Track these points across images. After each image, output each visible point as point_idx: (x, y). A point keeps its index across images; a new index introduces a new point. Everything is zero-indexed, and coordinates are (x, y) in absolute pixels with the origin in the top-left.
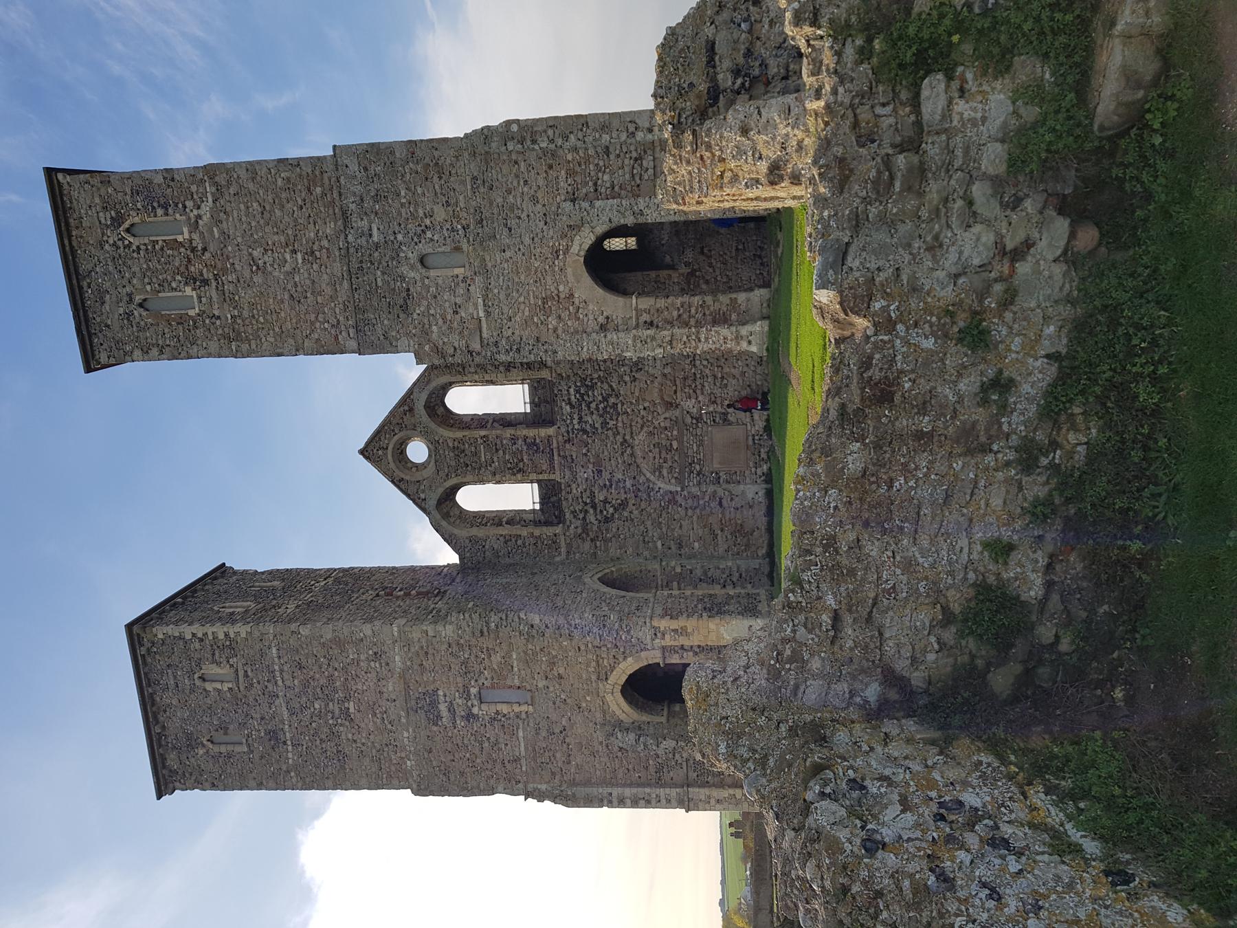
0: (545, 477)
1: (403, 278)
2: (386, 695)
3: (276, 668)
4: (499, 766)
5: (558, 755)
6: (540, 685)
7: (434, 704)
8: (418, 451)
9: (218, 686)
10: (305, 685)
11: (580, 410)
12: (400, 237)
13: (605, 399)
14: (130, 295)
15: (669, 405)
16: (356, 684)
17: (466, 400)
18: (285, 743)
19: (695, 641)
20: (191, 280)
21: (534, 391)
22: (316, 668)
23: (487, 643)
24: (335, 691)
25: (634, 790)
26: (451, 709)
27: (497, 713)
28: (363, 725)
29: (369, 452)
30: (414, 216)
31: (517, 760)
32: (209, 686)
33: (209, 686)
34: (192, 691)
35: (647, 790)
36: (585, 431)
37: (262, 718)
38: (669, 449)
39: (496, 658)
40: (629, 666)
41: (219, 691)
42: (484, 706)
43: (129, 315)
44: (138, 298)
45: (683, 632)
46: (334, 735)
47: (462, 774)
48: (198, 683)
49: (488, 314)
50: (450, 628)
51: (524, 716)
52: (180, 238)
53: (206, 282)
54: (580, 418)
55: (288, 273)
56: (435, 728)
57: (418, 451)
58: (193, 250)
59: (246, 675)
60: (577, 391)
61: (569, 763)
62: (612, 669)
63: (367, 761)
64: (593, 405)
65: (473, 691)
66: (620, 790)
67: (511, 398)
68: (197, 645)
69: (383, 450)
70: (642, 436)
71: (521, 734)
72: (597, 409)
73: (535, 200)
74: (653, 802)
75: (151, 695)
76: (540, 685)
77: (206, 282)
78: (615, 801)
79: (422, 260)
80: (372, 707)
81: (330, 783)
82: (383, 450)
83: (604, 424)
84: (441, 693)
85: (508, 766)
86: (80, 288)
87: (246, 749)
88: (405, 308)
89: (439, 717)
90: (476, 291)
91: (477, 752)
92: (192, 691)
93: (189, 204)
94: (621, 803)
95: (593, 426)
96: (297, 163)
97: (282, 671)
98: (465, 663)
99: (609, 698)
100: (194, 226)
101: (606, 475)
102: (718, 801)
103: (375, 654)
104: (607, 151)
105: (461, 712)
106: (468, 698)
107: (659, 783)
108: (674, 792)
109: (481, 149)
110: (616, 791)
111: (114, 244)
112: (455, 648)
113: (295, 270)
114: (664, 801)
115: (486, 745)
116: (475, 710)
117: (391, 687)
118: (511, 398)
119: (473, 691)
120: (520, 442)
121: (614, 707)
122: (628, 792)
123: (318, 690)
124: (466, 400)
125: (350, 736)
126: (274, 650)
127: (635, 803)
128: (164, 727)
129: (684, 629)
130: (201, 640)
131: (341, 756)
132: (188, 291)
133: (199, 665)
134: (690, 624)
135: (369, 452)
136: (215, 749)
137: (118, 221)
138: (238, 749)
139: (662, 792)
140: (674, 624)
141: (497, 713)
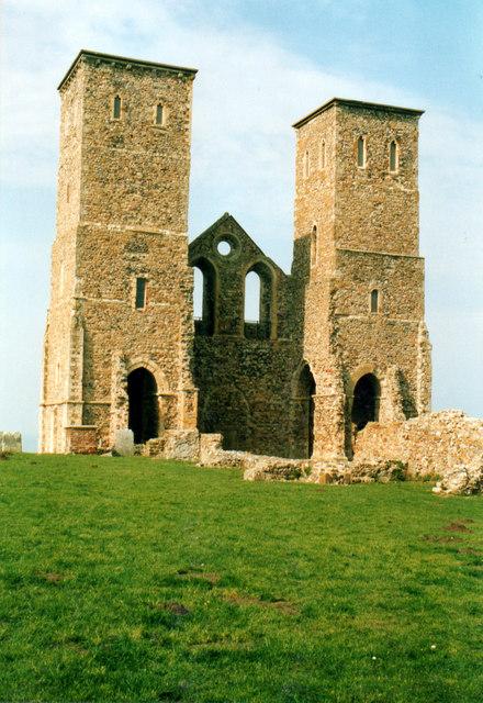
0: (216, 329)
1: (369, 280)
6: (149, 318)
7: (137, 249)
8: (224, 248)
9: (155, 115)
11: (254, 354)
13: (259, 370)
15: (253, 406)
17: (252, 283)
18: (115, 146)
20: (370, 169)
21: (258, 326)
22: (164, 179)
23: (176, 288)
24: (149, 188)
25: (81, 369)
26: (134, 259)
27: (131, 288)
29: (227, 221)
31: (99, 295)
32: (155, 108)
34: (152, 97)
35: (81, 377)
36: (242, 355)
38: (227, 404)
41: (152, 114)
42: (135, 280)
44: (364, 137)
45: (190, 407)
48: (158, 102)
51: (129, 304)
53: (369, 176)
57: (224, 248)
59: (161, 135)
60: (264, 354)
67: (252, 313)
68: (181, 109)
69: (226, 227)
70: (235, 390)
75: (151, 70)
76: (149, 318)
78: (74, 356)
82: (226, 227)
83: (245, 368)
85: (96, 289)
88: (355, 278)
89: (130, 251)
92: (152, 97)
94: (74, 360)
95: (244, 360)
101: (215, 365)
105: (133, 265)
106: (142, 272)
108: (79, 393)
110: (80, 357)
111: (388, 134)
116: (133, 274)
117: (148, 226)
118: (252, 313)
119: (146, 276)
120: (236, 315)
122: (80, 365)
124: (252, 283)
126: (175, 156)
127: (74, 369)
131: (105, 182)
132: (365, 166)
133: (170, 106)
135: (227, 221)
136: (113, 100)
137: (398, 139)
138: (112, 114)
139: (80, 386)
141: (131, 288)
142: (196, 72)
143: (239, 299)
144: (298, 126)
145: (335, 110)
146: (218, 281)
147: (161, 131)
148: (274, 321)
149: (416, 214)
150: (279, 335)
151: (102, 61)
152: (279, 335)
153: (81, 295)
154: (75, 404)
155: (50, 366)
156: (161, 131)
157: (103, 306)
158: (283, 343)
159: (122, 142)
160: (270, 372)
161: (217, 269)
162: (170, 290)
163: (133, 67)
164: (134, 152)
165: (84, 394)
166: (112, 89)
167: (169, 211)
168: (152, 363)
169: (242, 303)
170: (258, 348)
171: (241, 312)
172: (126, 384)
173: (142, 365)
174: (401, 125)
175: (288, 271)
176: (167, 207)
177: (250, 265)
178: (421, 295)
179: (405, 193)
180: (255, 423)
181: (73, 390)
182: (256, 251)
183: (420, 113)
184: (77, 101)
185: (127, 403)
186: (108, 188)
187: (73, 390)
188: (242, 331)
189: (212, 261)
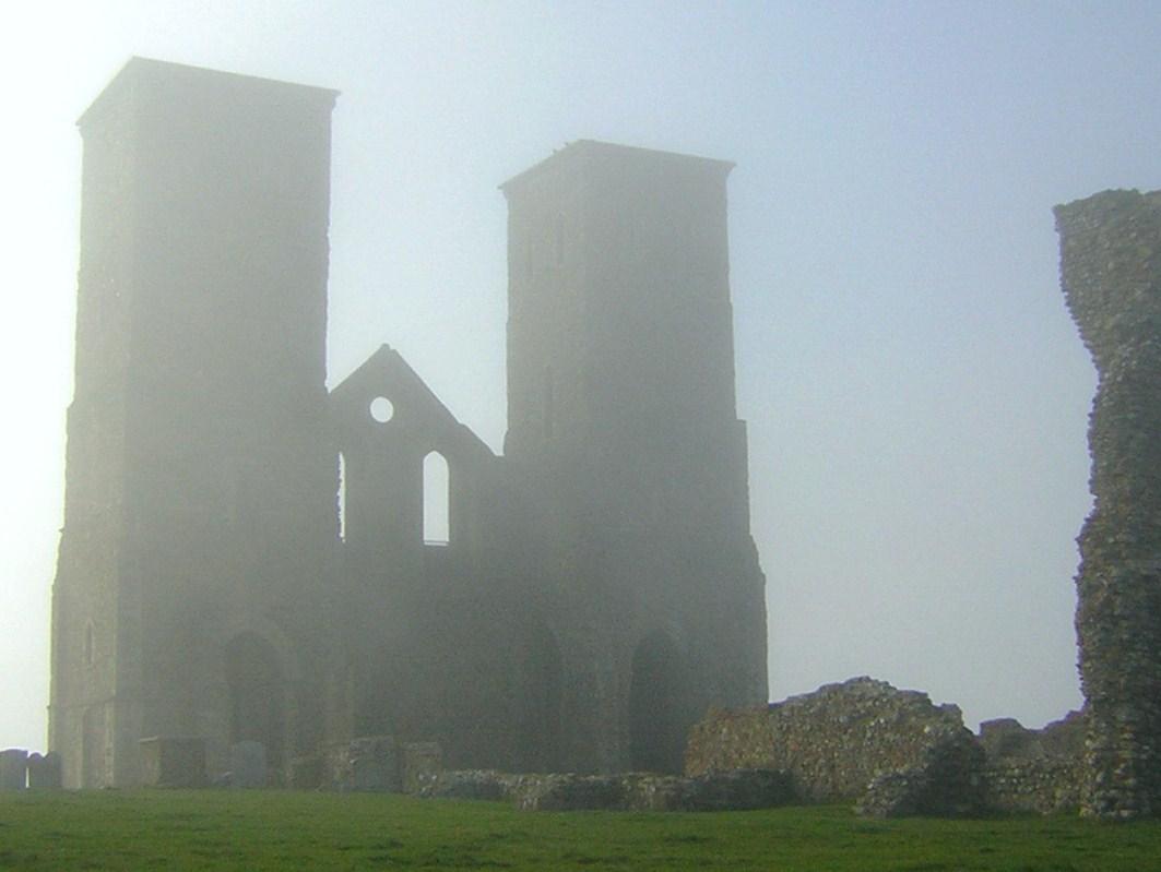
8: (382, 410)
17: (436, 471)
57: (382, 410)
67: (436, 527)
69: (387, 371)
82: (387, 371)
118: (436, 527)
124: (436, 471)
175: (498, 451)
182: (443, 415)
183: (734, 165)
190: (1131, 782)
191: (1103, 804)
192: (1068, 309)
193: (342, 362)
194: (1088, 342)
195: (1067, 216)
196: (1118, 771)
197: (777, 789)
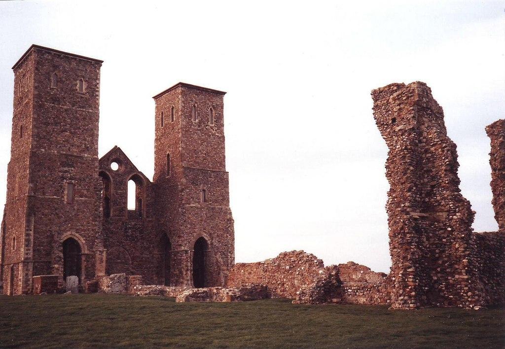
0: (111, 215)
1: (200, 184)
2: (71, 147)
3: (84, 110)
4: (42, 186)
5: (47, 211)
8: (115, 166)
10: (77, 118)
12: (209, 185)
14: (197, 103)
16: (76, 137)
17: (132, 186)
18: (53, 103)
19: (98, 266)
20: (200, 122)
23: (92, 189)
24: (75, 129)
25: (32, 240)
26: (66, 171)
27: (64, 189)
28: (59, 136)
30: (214, 191)
31: (44, 194)
32: (78, 82)
33: (78, 82)
35: (32, 245)
37: (64, 98)
39: (85, 192)
40: (82, 241)
41: (76, 85)
43: (192, 100)
44: (196, 105)
46: (56, 124)
47: (39, 171)
49: (192, 207)
50: (97, 176)
51: (63, 199)
52: (209, 123)
53: (199, 126)
54: (130, 228)
55: (201, 151)
56: (59, 164)
57: (115, 166)
58: (207, 125)
59: (81, 97)
61: (43, 215)
62: (81, 235)
63: (44, 134)
64: (134, 233)
65: (73, 181)
66: (32, 234)
67: (131, 205)
68: (94, 83)
69: (117, 154)
71: (55, 197)
72: (133, 234)
73: (217, 224)
74: (27, 248)
75: (75, 59)
76: (76, 207)
77: (199, 126)
79: (204, 191)
80: (67, 141)
81: (36, 116)
82: (117, 154)
83: (127, 236)
84: (72, 169)
86: (199, 90)
87: (52, 87)
88: (193, 183)
90: (197, 205)
91: (49, 178)
93: (216, 128)
94: (28, 235)
96: (225, 161)
97: (83, 111)
98: (84, 180)
99: (69, 233)
100: (212, 128)
102: (27, 274)
103: (88, 147)
104: (226, 245)
106: (70, 179)
107: (34, 251)
108: (30, 256)
109: (229, 212)
110: (32, 233)
112: (90, 177)
113: (202, 153)
114: (27, 252)
115: (51, 183)
116: (65, 181)
117: (75, 151)
118: (131, 205)
119: (73, 181)
120: (123, 205)
121: (65, 234)
122: (32, 238)
123: (74, 123)
124: (132, 186)
125: (56, 130)
127: (27, 240)
128: (61, 58)
129: (102, 262)
130: (96, 86)
132: (197, 121)
134: (104, 264)
137: (213, 106)
139: (31, 251)
140: (104, 259)
141: (64, 189)
142: (102, 62)
143: (124, 196)
144: (155, 98)
145: (179, 90)
146: (112, 186)
147: (82, 95)
148: (144, 208)
149: (223, 148)
150: (148, 217)
151: (45, 52)
152: (148, 217)
153: (33, 194)
154: (28, 263)
155: (7, 241)
156: (82, 95)
157: (47, 200)
158: (149, 221)
159: (59, 101)
160: (142, 238)
161: (110, 176)
162: (88, 190)
163: (64, 56)
164: (65, 107)
165: (34, 256)
166: (51, 68)
167: (86, 142)
168: (77, 235)
169: (126, 198)
170: (136, 225)
171: (126, 203)
172: (62, 248)
173: (70, 236)
174: (216, 100)
175: (151, 180)
176: (85, 140)
177: (130, 176)
178: (228, 193)
179: (218, 136)
180: (134, 269)
181: (27, 254)
182: (133, 168)
183: (224, 93)
184: (28, 75)
185: (63, 260)
186: (50, 128)
187: (27, 254)
188: (126, 215)
189: (108, 173)
190: (413, 293)
191: (403, 302)
192: (377, 125)
193: (103, 150)
194: (384, 137)
195: (377, 95)
196: (408, 290)
197: (261, 293)
